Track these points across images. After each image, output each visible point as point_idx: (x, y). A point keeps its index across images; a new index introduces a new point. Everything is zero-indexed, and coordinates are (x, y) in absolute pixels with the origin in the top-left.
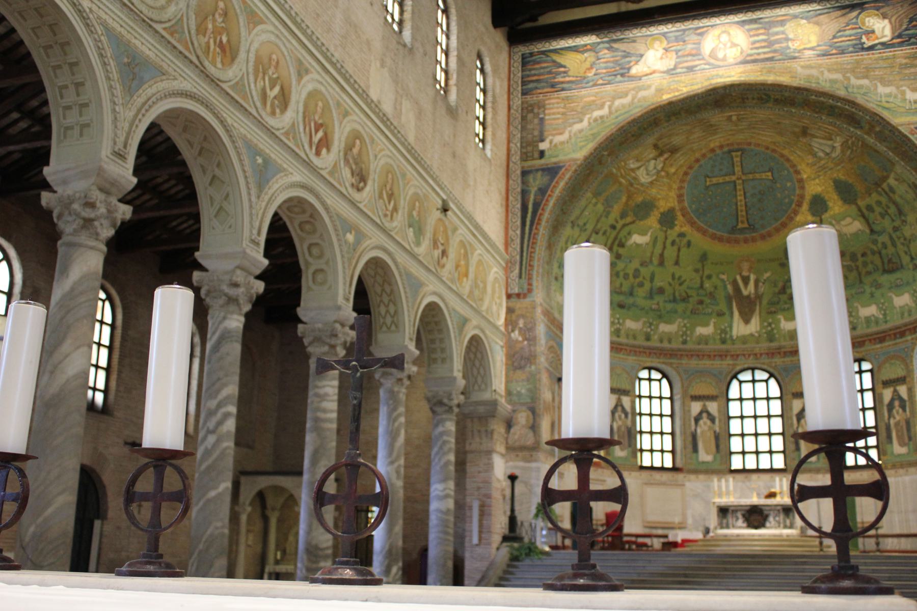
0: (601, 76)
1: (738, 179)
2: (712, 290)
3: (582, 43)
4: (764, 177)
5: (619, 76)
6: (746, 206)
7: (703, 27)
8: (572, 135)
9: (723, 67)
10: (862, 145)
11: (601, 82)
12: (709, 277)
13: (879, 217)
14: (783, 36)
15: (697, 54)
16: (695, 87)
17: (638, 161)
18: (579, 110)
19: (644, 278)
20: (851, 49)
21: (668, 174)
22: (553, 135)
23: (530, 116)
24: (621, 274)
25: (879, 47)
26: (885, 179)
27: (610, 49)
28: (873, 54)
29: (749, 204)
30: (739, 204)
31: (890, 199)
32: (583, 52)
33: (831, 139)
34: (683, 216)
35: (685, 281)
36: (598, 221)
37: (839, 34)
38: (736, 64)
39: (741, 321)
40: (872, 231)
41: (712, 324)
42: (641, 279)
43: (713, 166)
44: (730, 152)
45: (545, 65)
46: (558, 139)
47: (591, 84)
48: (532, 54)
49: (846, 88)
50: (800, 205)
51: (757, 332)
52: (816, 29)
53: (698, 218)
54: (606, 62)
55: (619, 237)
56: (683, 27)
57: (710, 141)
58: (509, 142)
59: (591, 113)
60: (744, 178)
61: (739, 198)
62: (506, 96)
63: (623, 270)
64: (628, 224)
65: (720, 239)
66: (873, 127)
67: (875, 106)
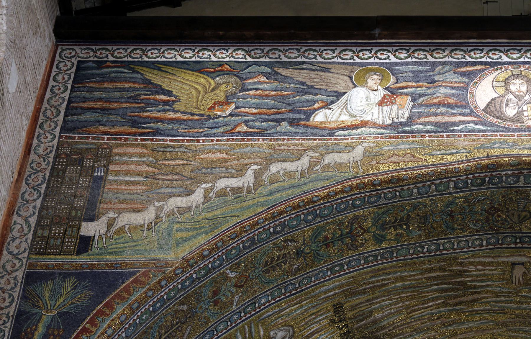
3: (213, 59)
7: (474, 64)
8: (162, 215)
9: (514, 130)
11: (245, 128)
16: (451, 158)
22: (120, 212)
32: (212, 74)
45: (127, 86)
47: (221, 130)
48: (100, 64)
54: (261, 96)
56: (431, 59)
58: (10, 213)
59: (214, 181)
62: (26, 123)
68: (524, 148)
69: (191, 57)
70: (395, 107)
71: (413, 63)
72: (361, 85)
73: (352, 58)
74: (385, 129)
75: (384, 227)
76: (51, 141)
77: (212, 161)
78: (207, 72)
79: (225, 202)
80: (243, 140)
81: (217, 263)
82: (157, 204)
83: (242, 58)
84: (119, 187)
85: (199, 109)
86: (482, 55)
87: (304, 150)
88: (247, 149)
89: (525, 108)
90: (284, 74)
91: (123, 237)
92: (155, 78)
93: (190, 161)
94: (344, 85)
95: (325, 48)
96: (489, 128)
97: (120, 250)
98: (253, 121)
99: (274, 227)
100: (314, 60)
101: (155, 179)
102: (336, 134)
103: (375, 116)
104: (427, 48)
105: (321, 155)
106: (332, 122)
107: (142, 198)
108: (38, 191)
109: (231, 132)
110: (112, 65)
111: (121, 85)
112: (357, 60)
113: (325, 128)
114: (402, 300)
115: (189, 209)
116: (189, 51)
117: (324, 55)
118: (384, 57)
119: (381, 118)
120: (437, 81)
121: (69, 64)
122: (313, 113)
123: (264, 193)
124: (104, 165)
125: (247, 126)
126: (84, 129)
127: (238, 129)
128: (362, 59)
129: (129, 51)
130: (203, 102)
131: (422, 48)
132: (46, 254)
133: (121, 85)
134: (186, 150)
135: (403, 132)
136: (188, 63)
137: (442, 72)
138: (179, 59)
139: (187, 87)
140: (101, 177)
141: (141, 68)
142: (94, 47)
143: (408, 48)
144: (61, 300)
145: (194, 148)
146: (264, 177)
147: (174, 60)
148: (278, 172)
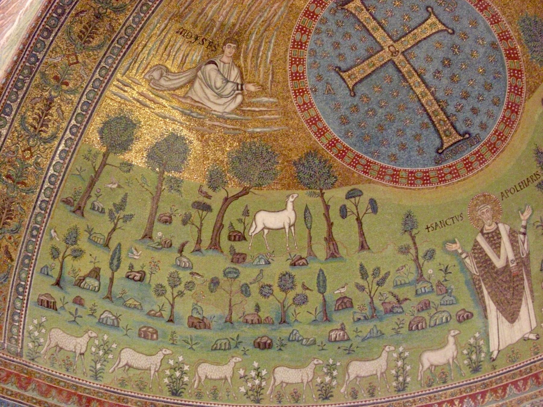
1: (394, 53)
2: (441, 276)
6: (438, 101)
12: (430, 255)
19: (304, 286)
24: (254, 289)
29: (440, 94)
30: (424, 101)
34: (342, 157)
35: (388, 274)
36: (156, 199)
39: (502, 319)
41: (451, 340)
42: (299, 289)
43: (336, 46)
51: (530, 333)
53: (372, 154)
60: (399, 47)
61: (418, 91)
63: (255, 281)
64: (236, 197)
65: (426, 179)
81: (33, 59)
99: (55, 11)
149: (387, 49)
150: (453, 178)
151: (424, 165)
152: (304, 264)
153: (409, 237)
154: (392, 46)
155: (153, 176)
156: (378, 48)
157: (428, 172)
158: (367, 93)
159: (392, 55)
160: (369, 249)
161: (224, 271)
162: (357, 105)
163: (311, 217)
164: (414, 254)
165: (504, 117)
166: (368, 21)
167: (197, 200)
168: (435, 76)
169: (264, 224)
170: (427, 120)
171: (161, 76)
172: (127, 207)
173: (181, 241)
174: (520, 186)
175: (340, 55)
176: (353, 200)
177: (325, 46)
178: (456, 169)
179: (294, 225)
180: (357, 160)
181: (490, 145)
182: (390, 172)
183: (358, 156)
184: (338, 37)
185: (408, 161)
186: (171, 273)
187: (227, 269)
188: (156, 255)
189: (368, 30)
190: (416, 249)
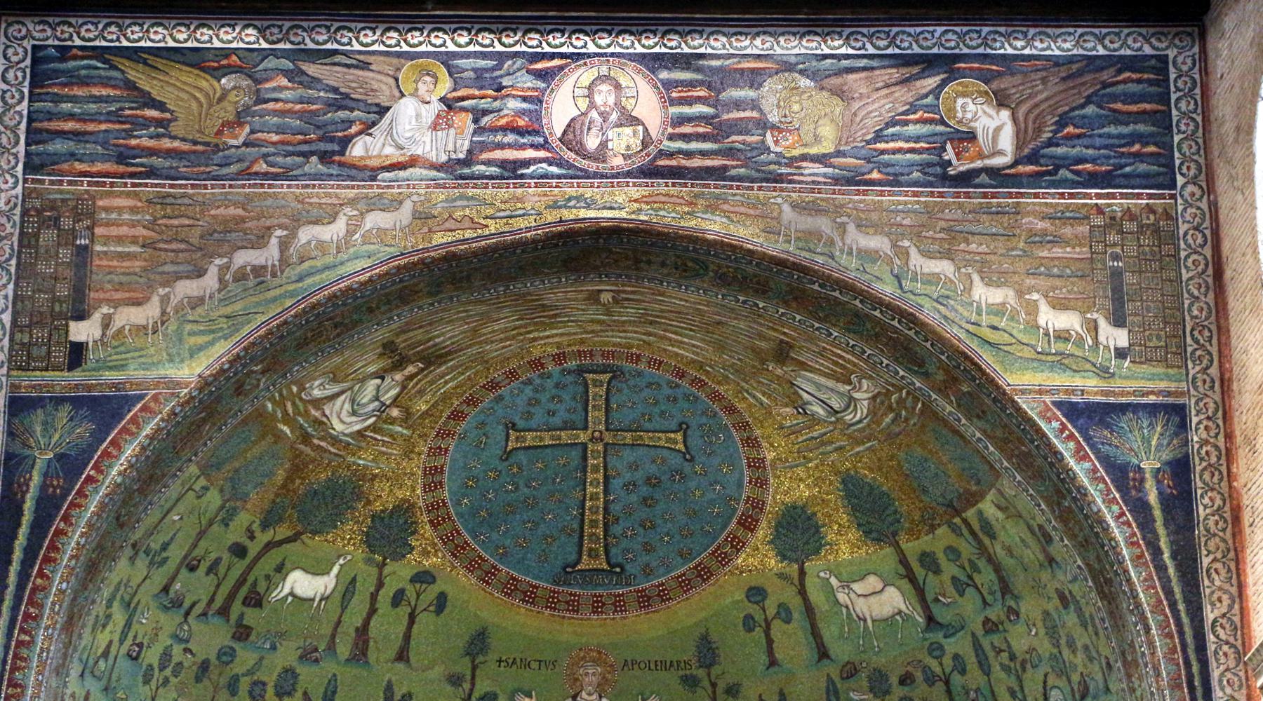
0: (264, 150)
3: (217, 44)
4: (662, 443)
5: (314, 159)
7: (552, 56)
8: (169, 310)
9: (596, 175)
10: (922, 412)
11: (262, 167)
13: (951, 590)
14: (755, 114)
15: (531, 130)
17: (335, 380)
18: (195, 241)
20: (916, 175)
21: (408, 413)
22: (116, 304)
23: (48, 237)
24: (244, 684)
25: (983, 178)
26: (972, 499)
27: (295, 75)
28: (967, 195)
29: (616, 508)
30: (588, 504)
31: (982, 550)
33: (850, 383)
36: (201, 534)
37: (891, 130)
38: (629, 174)
40: (930, 619)
44: (580, 371)
45: (104, 92)
46: (128, 316)
47: (234, 169)
48: (64, 52)
49: (897, 277)
50: (749, 524)
52: (837, 107)
53: (475, 537)
54: (282, 113)
55: (251, 579)
56: (499, 48)
57: (535, 339)
59: (230, 255)
60: (608, 438)
61: (590, 490)
63: (250, 673)
65: (529, 596)
66: (955, 380)
67: (963, 336)
68: (604, 208)
69: (186, 41)
70: (452, 131)
71: (476, 55)
72: (411, 95)
73: (398, 45)
74: (439, 171)
75: (438, 285)
76: (14, 188)
77: (225, 221)
78: (209, 67)
79: (245, 290)
80: (262, 186)
82: (162, 291)
83: (254, 43)
84: (111, 263)
85: (203, 133)
86: (563, 40)
87: (341, 205)
88: (269, 202)
89: (610, 134)
90: (310, 73)
91: (123, 344)
92: (140, 79)
93: (198, 220)
94: (387, 93)
95: (363, 25)
96: (564, 172)
97: (121, 363)
98: (274, 154)
100: (348, 48)
101: (155, 249)
102: (379, 177)
103: (428, 148)
104: (493, 27)
105: (362, 214)
106: (375, 157)
107: (141, 280)
108: (7, 270)
109: (246, 174)
110: (80, 53)
111: (96, 91)
112: (405, 48)
113: (365, 168)
114: (467, 323)
115: (201, 301)
116: (183, 29)
117: (362, 39)
118: (439, 42)
119: (434, 152)
120: (505, 87)
121: (20, 50)
122: (350, 141)
123: (294, 279)
124: (88, 227)
125: (266, 163)
126: (55, 167)
127: (256, 168)
128: (411, 46)
129: (100, 26)
130: (208, 121)
131: (487, 26)
132: (29, 370)
133: (96, 91)
134: (191, 201)
135: (462, 177)
136: (184, 51)
137: (511, 71)
138: (171, 44)
139: (185, 96)
140: (86, 247)
141: (118, 59)
142: (50, 20)
143: (469, 26)
144: (57, 436)
145: (200, 199)
146: (291, 250)
147: (162, 45)
148: (309, 242)
149: (589, 432)
150: (568, 610)
151: (540, 579)
152: (317, 661)
153: (470, 665)
154: (601, 432)
155: (219, 503)
156: (580, 426)
157: (537, 588)
158: (525, 463)
159: (591, 440)
160: (408, 661)
161: (220, 651)
162: (500, 472)
163: (354, 593)
164: (467, 691)
165: (684, 575)
166: (598, 398)
167: (238, 540)
168: (625, 485)
169: (292, 588)
170: (576, 526)
171: (321, 384)
172: (172, 547)
173: (195, 598)
174: (656, 665)
175: (529, 412)
176: (418, 586)
177: (519, 398)
178: (578, 601)
179: (328, 597)
180: (452, 535)
181: (642, 597)
182: (486, 567)
183: (458, 532)
184: (544, 398)
185: (519, 562)
186: (166, 648)
187: (225, 647)
188: (163, 618)
189: (587, 405)
190: (473, 684)
